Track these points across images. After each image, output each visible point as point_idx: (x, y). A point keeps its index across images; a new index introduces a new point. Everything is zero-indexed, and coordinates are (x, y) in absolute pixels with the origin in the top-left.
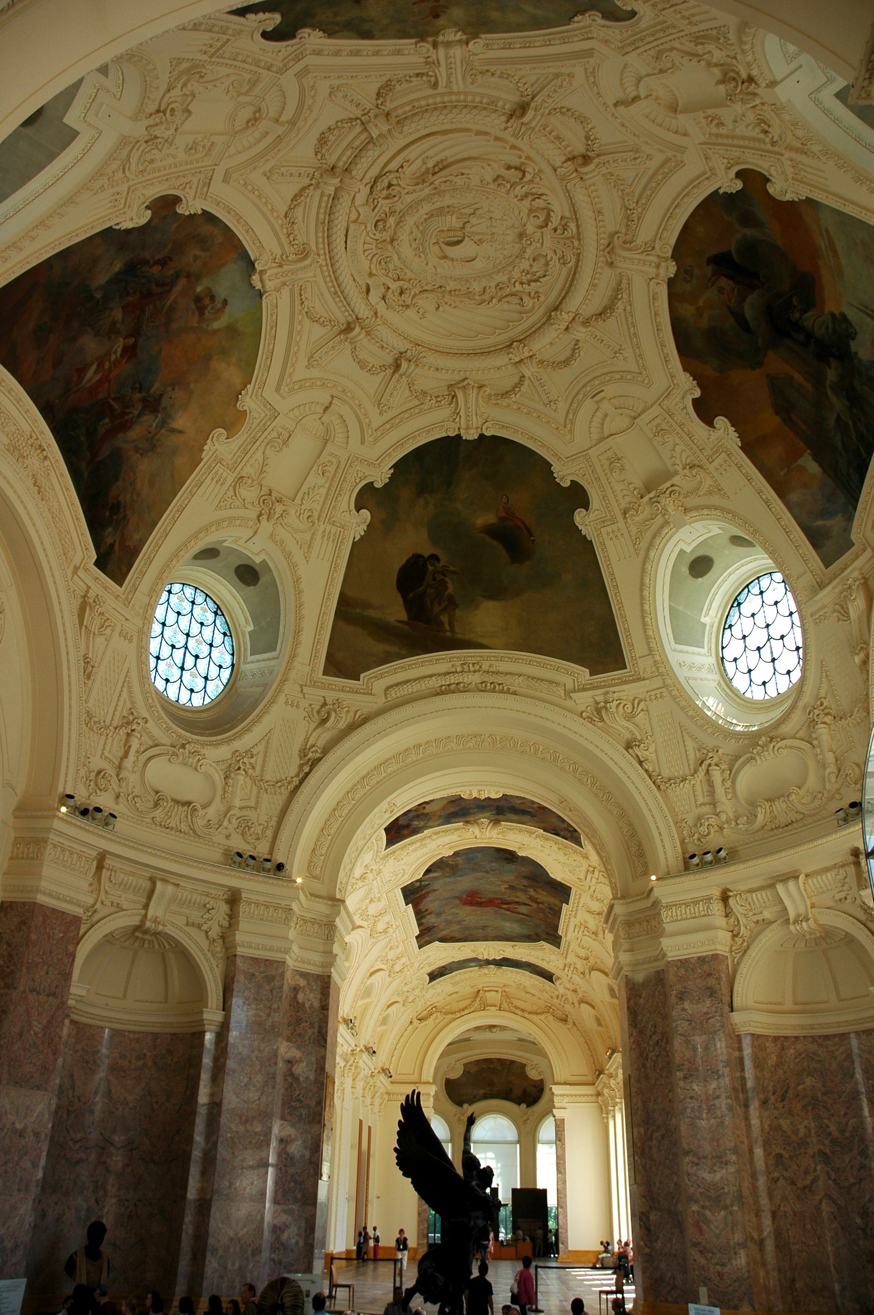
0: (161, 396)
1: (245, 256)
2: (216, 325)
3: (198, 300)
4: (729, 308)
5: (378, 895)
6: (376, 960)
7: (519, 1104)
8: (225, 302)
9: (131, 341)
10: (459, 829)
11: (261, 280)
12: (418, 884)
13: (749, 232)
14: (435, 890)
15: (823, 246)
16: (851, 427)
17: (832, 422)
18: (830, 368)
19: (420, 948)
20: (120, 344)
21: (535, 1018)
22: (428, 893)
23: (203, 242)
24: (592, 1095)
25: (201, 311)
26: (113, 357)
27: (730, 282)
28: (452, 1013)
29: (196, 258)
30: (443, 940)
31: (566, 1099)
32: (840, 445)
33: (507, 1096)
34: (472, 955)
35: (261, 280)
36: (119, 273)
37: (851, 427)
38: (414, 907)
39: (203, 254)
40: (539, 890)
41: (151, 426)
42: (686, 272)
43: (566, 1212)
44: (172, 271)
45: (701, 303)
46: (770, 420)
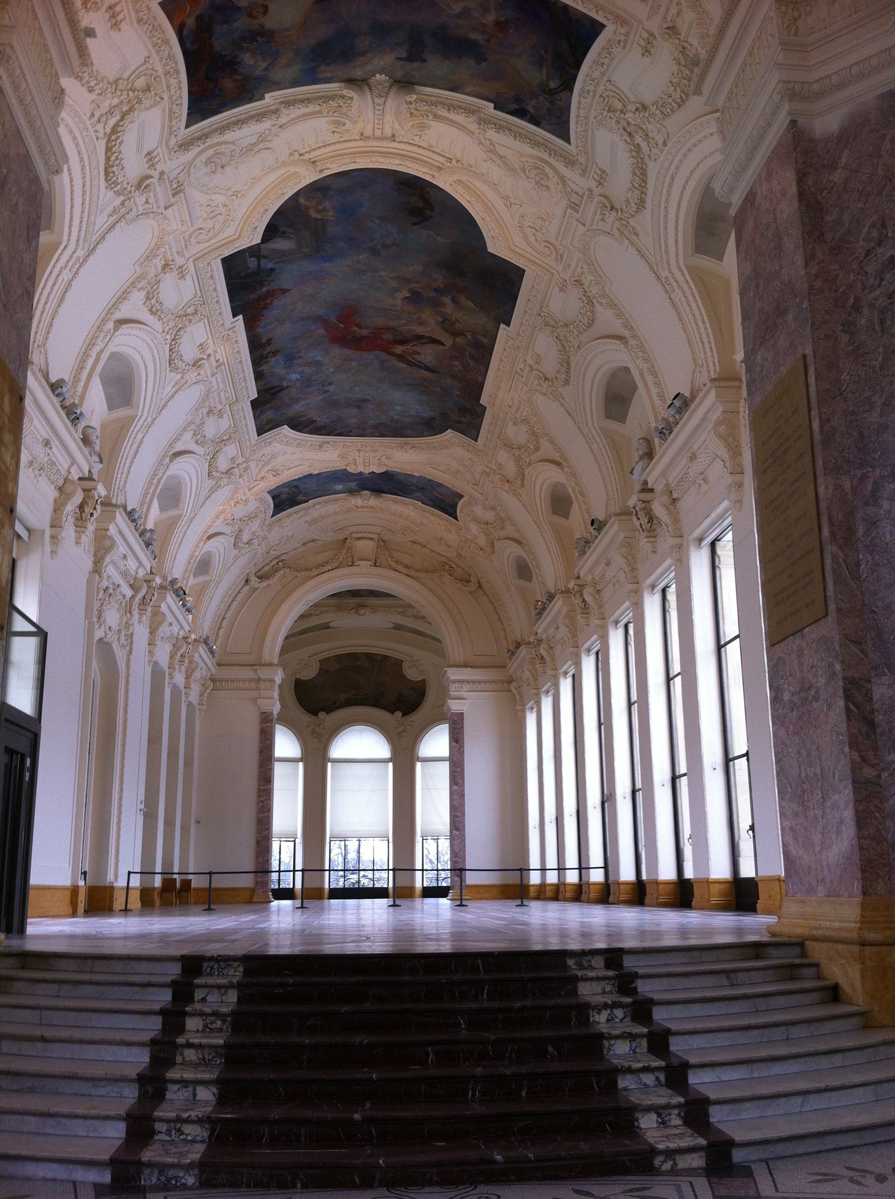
5: (180, 261)
6: (185, 429)
7: (393, 712)
10: (332, 98)
12: (252, 263)
14: (284, 291)
19: (260, 431)
21: (423, 575)
22: (271, 294)
24: (503, 682)
28: (307, 570)
30: (298, 425)
31: (466, 687)
33: (376, 702)
34: (339, 465)
38: (250, 326)
40: (462, 299)
43: (464, 836)
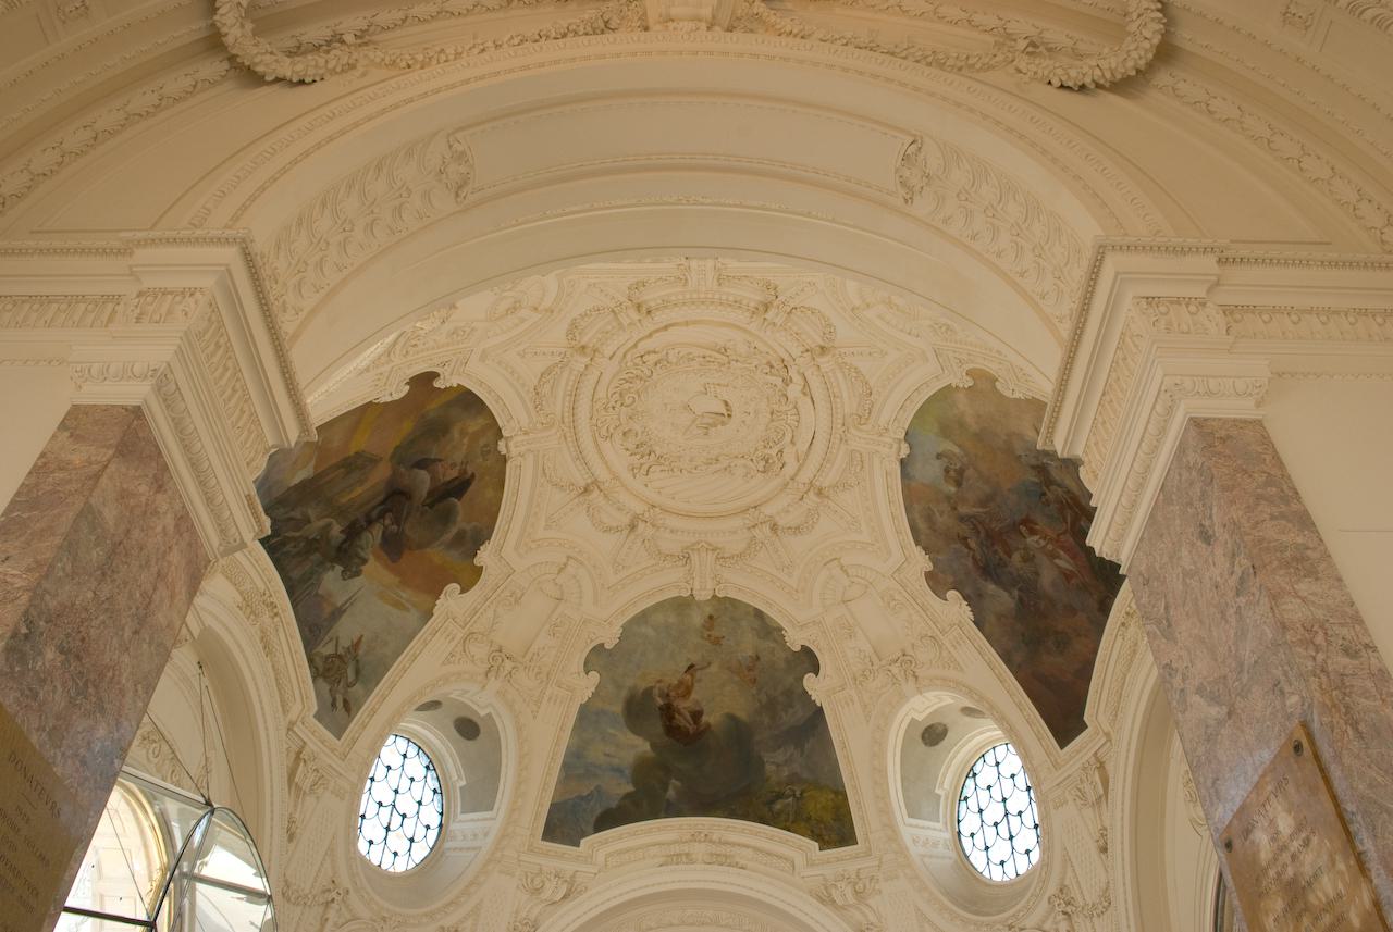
0: (1033, 467)
1: (905, 475)
2: (956, 450)
3: (959, 484)
4: (440, 460)
8: (939, 456)
9: (1023, 529)
11: (899, 449)
13: (454, 531)
15: (404, 595)
16: (297, 534)
17: (311, 513)
18: (342, 532)
20: (1032, 540)
23: (930, 519)
25: (961, 472)
26: (1043, 543)
27: (448, 478)
29: (942, 514)
32: (292, 514)
35: (899, 449)
36: (995, 583)
37: (297, 534)
39: (935, 510)
41: (1056, 467)
42: (489, 452)
44: (964, 526)
45: (465, 441)
46: (360, 443)
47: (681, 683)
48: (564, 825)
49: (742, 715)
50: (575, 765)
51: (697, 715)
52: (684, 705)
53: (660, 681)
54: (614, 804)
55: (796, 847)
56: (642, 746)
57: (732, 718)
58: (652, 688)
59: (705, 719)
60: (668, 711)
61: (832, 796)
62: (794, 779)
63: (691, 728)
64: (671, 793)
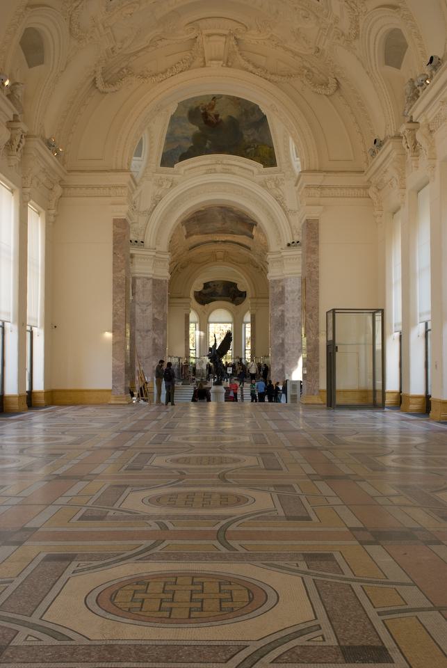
47: (210, 104)
48: (168, 160)
49: (235, 116)
50: (170, 137)
51: (217, 116)
52: (212, 113)
53: (202, 104)
54: (186, 151)
55: (255, 166)
56: (196, 129)
57: (230, 117)
58: (199, 106)
59: (220, 117)
60: (205, 115)
61: (268, 148)
62: (254, 141)
63: (215, 121)
64: (207, 146)
